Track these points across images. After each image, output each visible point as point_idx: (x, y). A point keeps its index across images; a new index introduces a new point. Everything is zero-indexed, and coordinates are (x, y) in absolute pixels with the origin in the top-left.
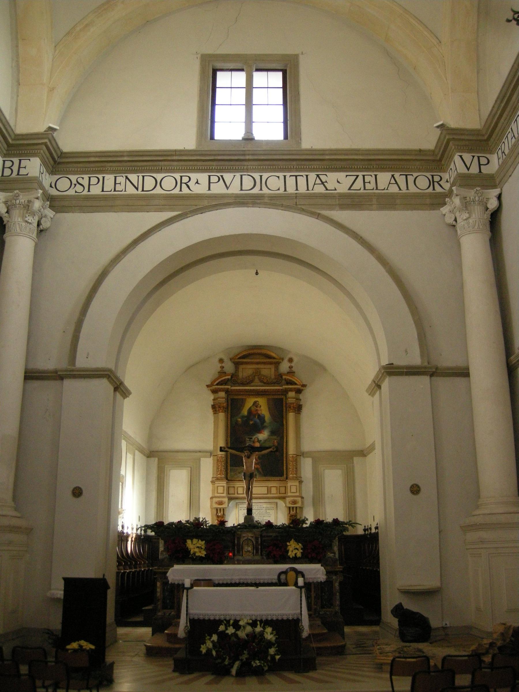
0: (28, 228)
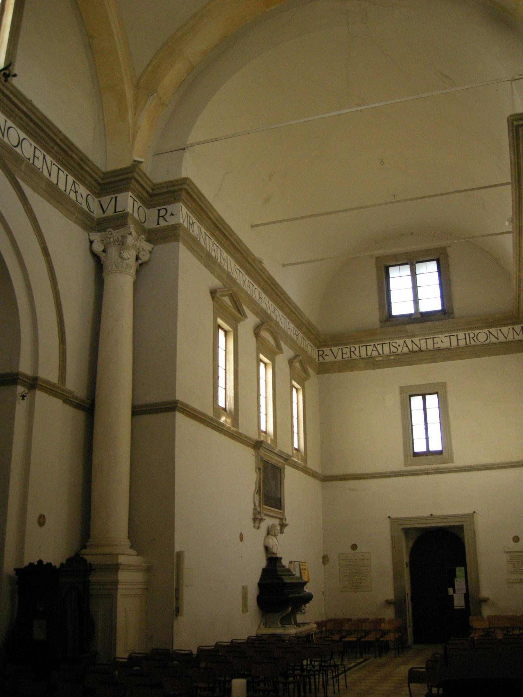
0: (125, 264)
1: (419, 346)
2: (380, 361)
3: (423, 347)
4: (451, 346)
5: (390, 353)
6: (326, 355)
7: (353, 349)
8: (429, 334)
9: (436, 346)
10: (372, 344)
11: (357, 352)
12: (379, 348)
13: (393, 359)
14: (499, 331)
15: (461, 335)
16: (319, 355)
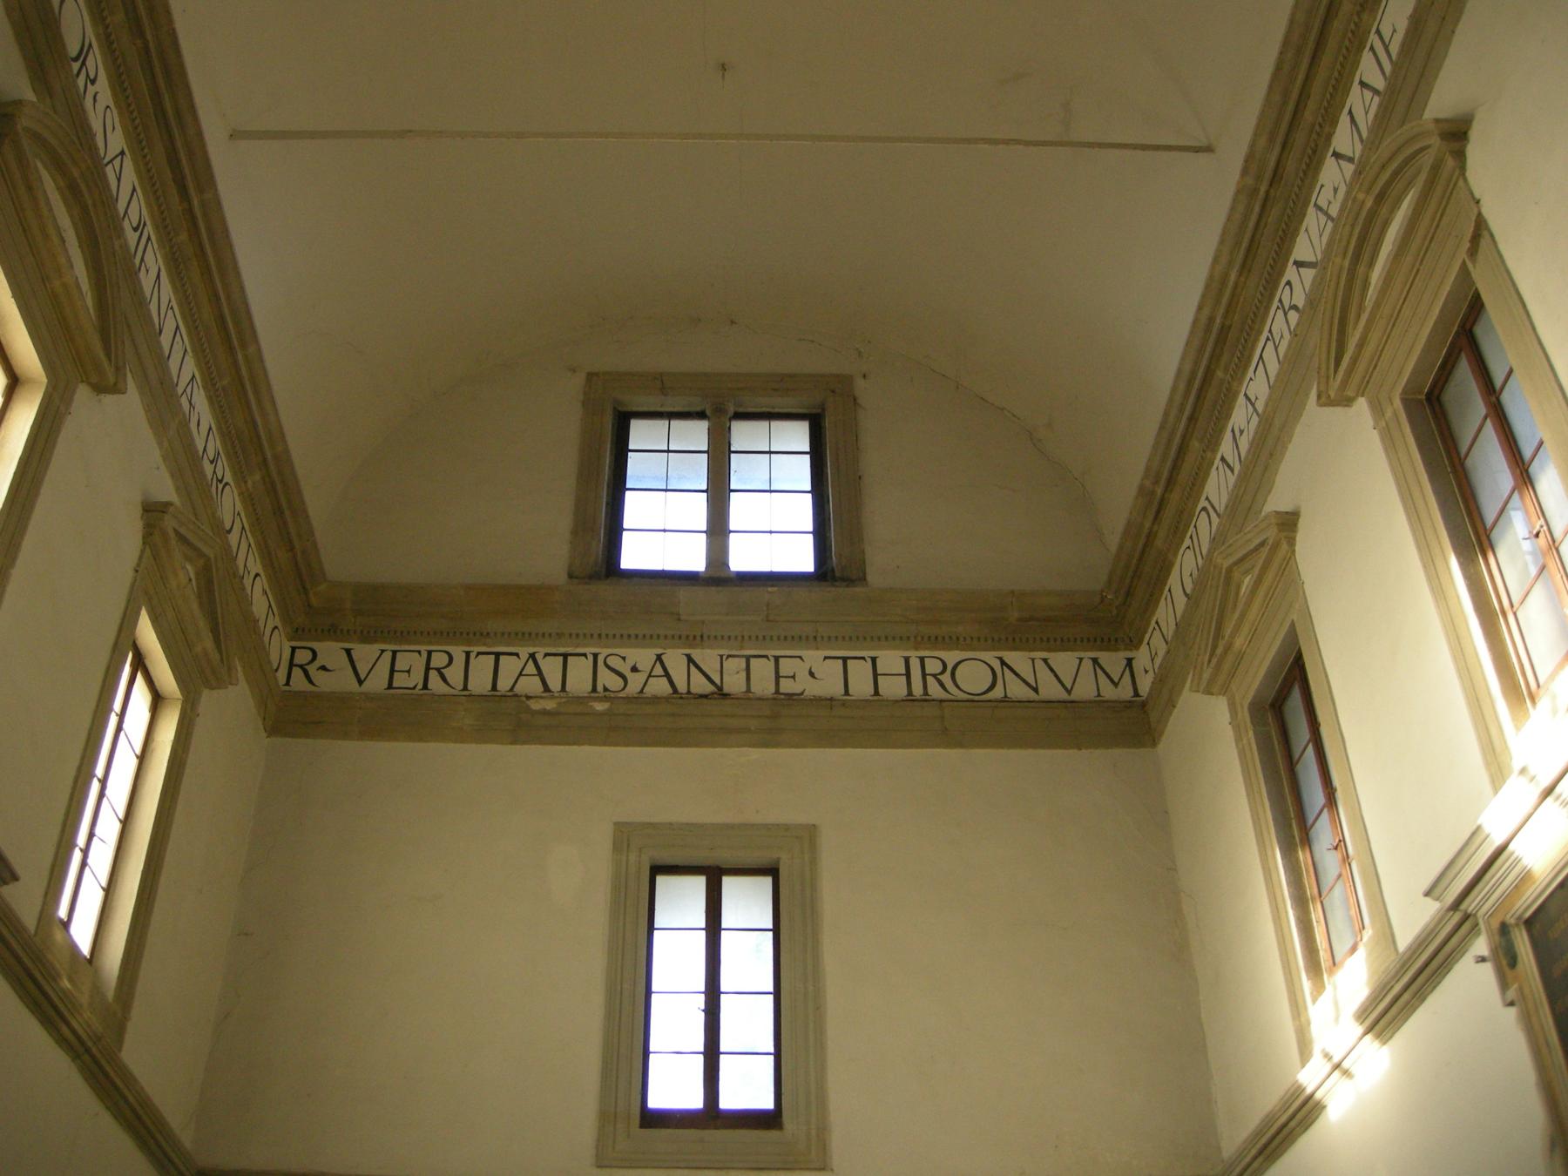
1: (718, 681)
2: (544, 712)
3: (734, 682)
4: (847, 693)
5: (594, 689)
6: (323, 668)
7: (439, 660)
8: (763, 640)
9: (787, 686)
10: (524, 652)
11: (455, 674)
12: (552, 668)
13: (601, 714)
14: (1040, 665)
15: (891, 660)
16: (291, 665)
